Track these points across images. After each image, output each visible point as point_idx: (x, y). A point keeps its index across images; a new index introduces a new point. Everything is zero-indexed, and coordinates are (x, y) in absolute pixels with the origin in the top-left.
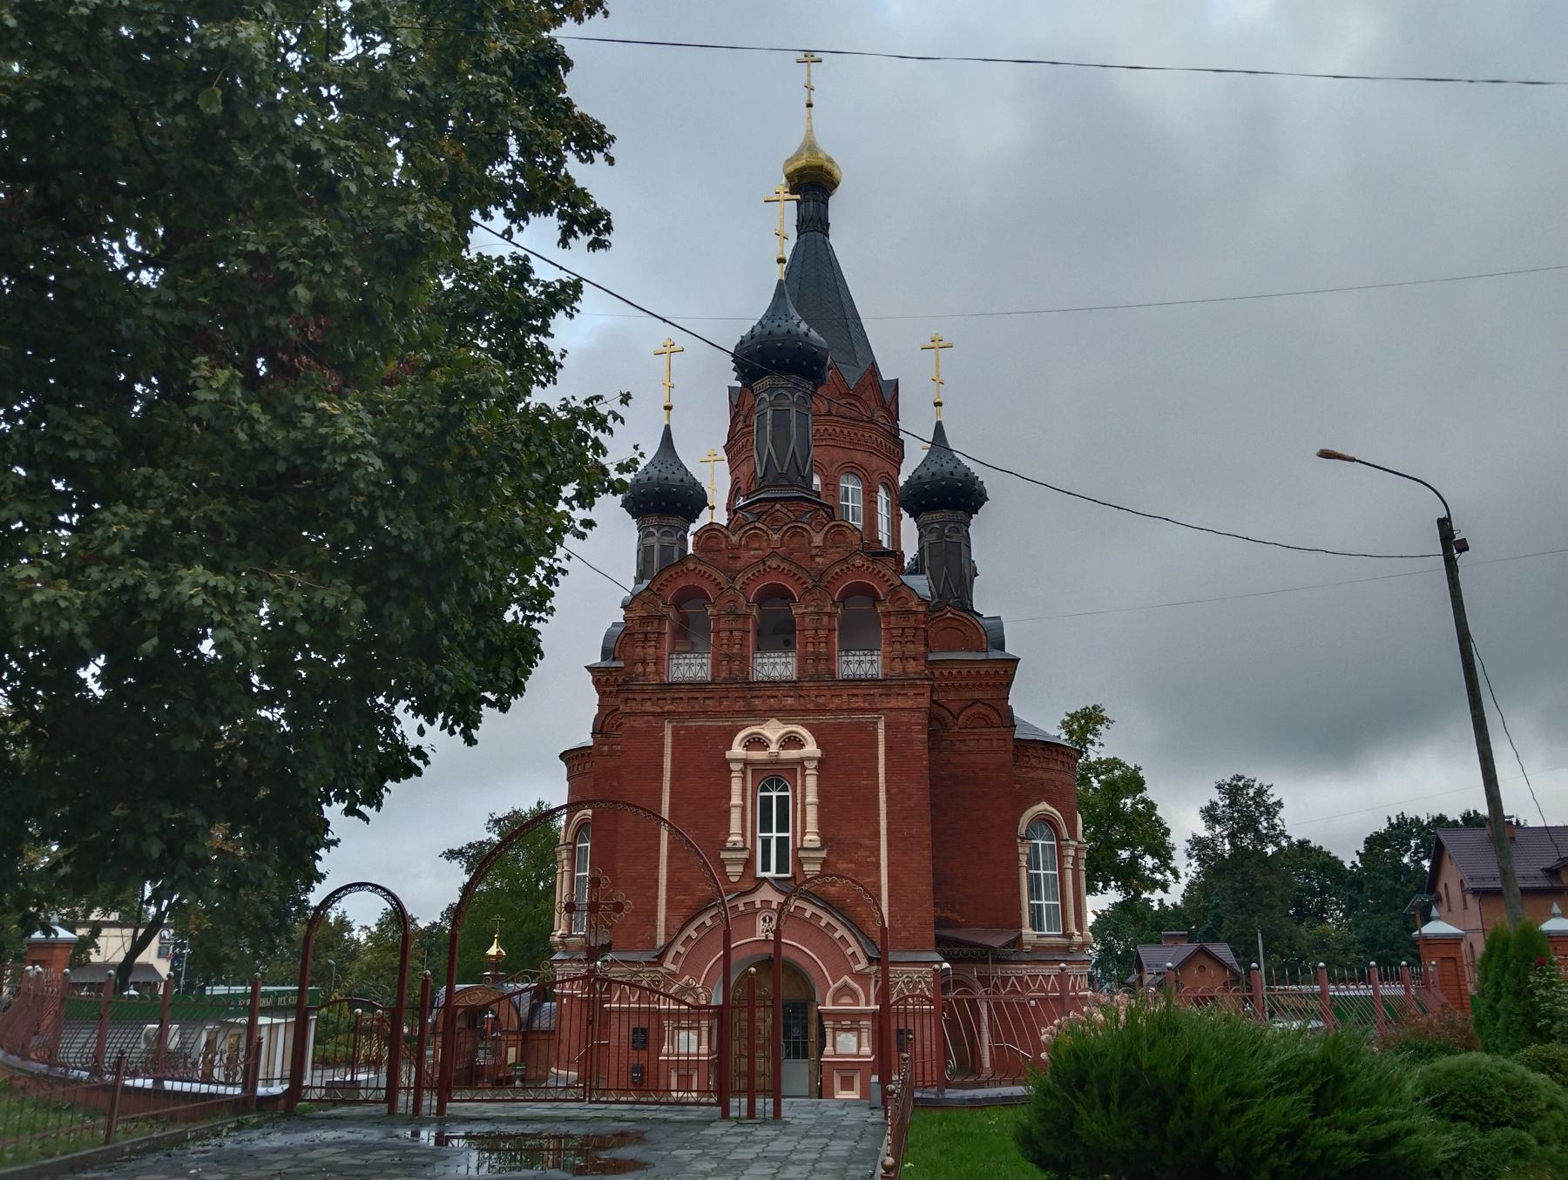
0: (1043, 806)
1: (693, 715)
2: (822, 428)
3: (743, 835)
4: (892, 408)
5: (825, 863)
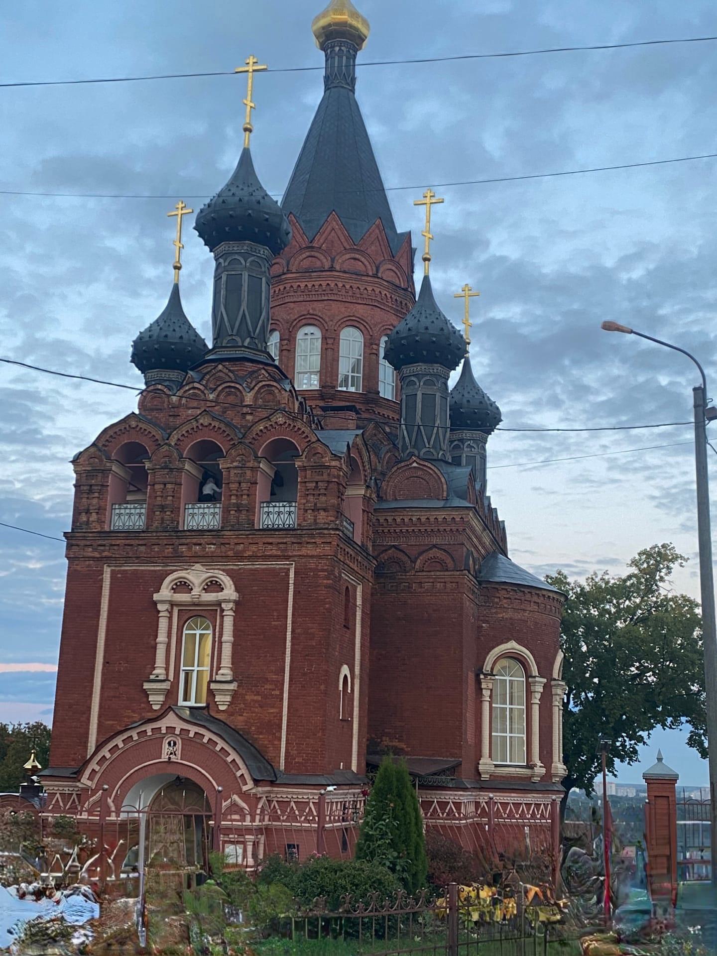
0: (512, 645)
1: (127, 559)
2: (324, 284)
3: (167, 669)
4: (403, 262)
5: (235, 695)
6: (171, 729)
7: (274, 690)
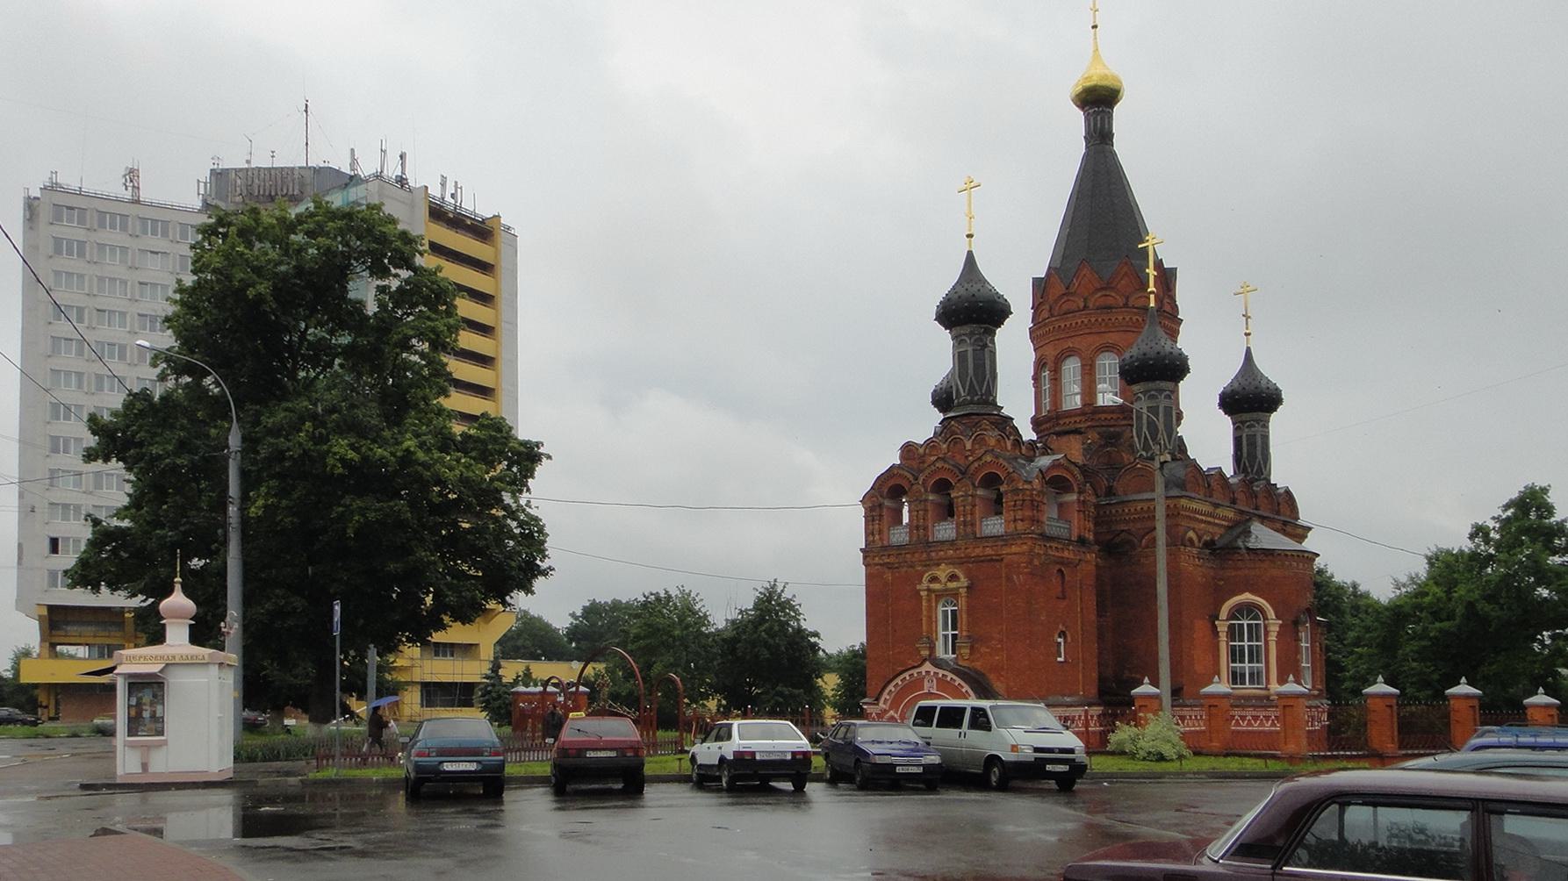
0: (1247, 597)
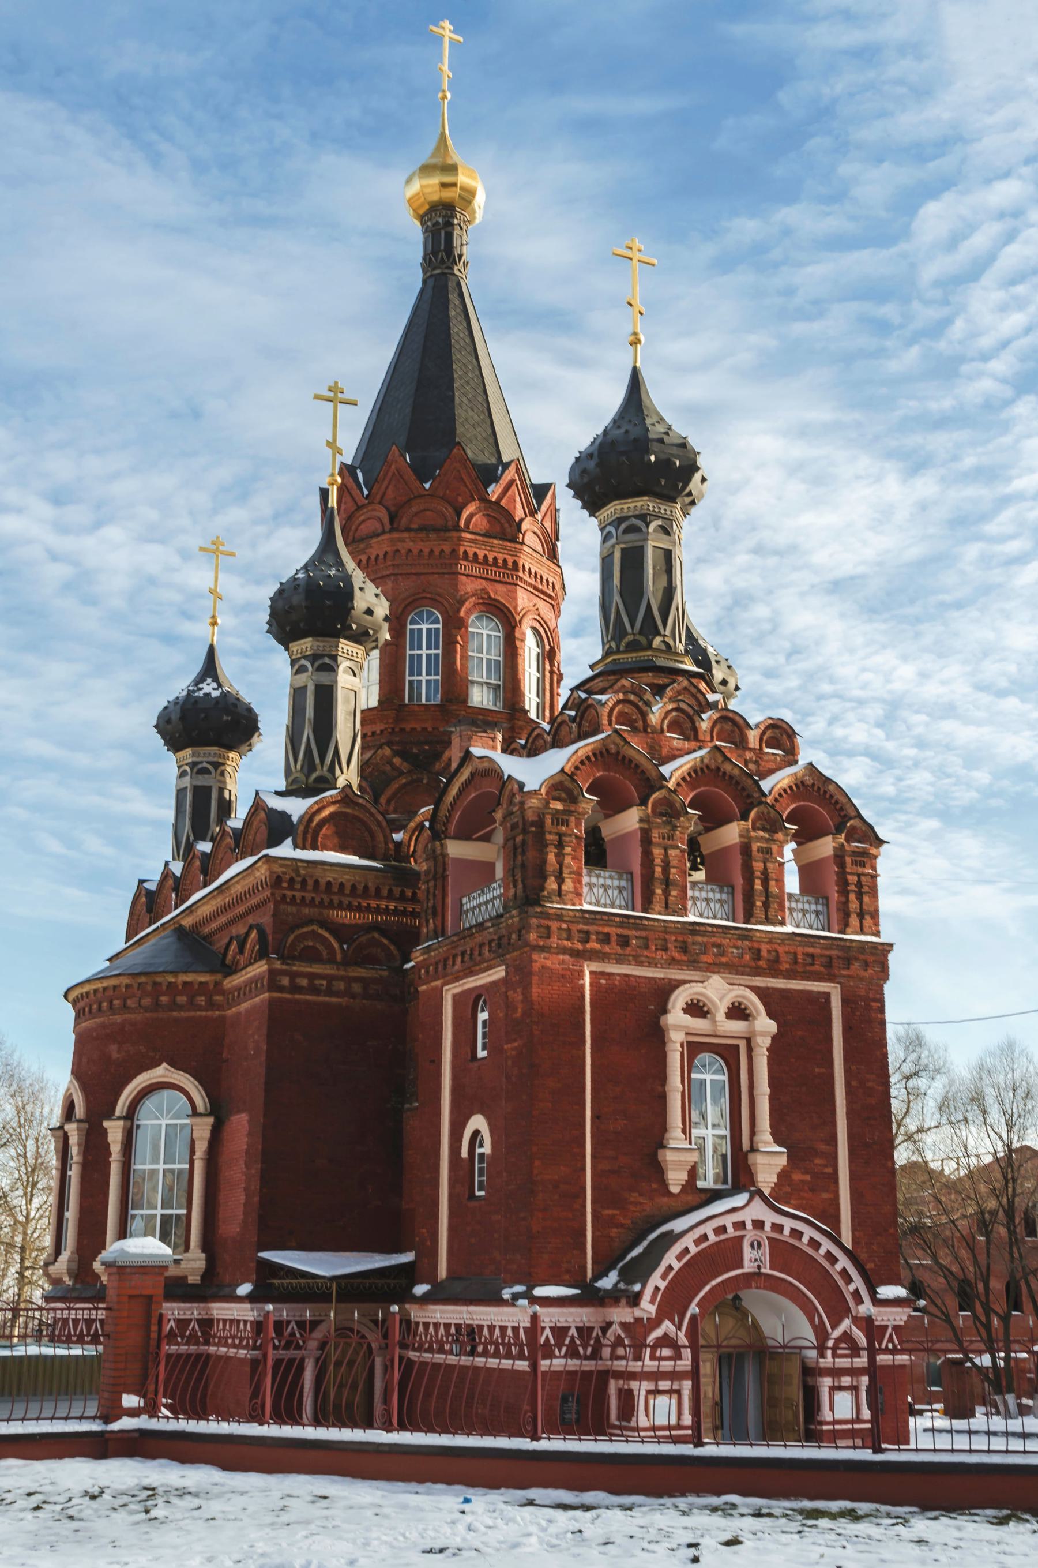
5: (783, 1175)
6: (759, 1224)
7: (826, 1166)
